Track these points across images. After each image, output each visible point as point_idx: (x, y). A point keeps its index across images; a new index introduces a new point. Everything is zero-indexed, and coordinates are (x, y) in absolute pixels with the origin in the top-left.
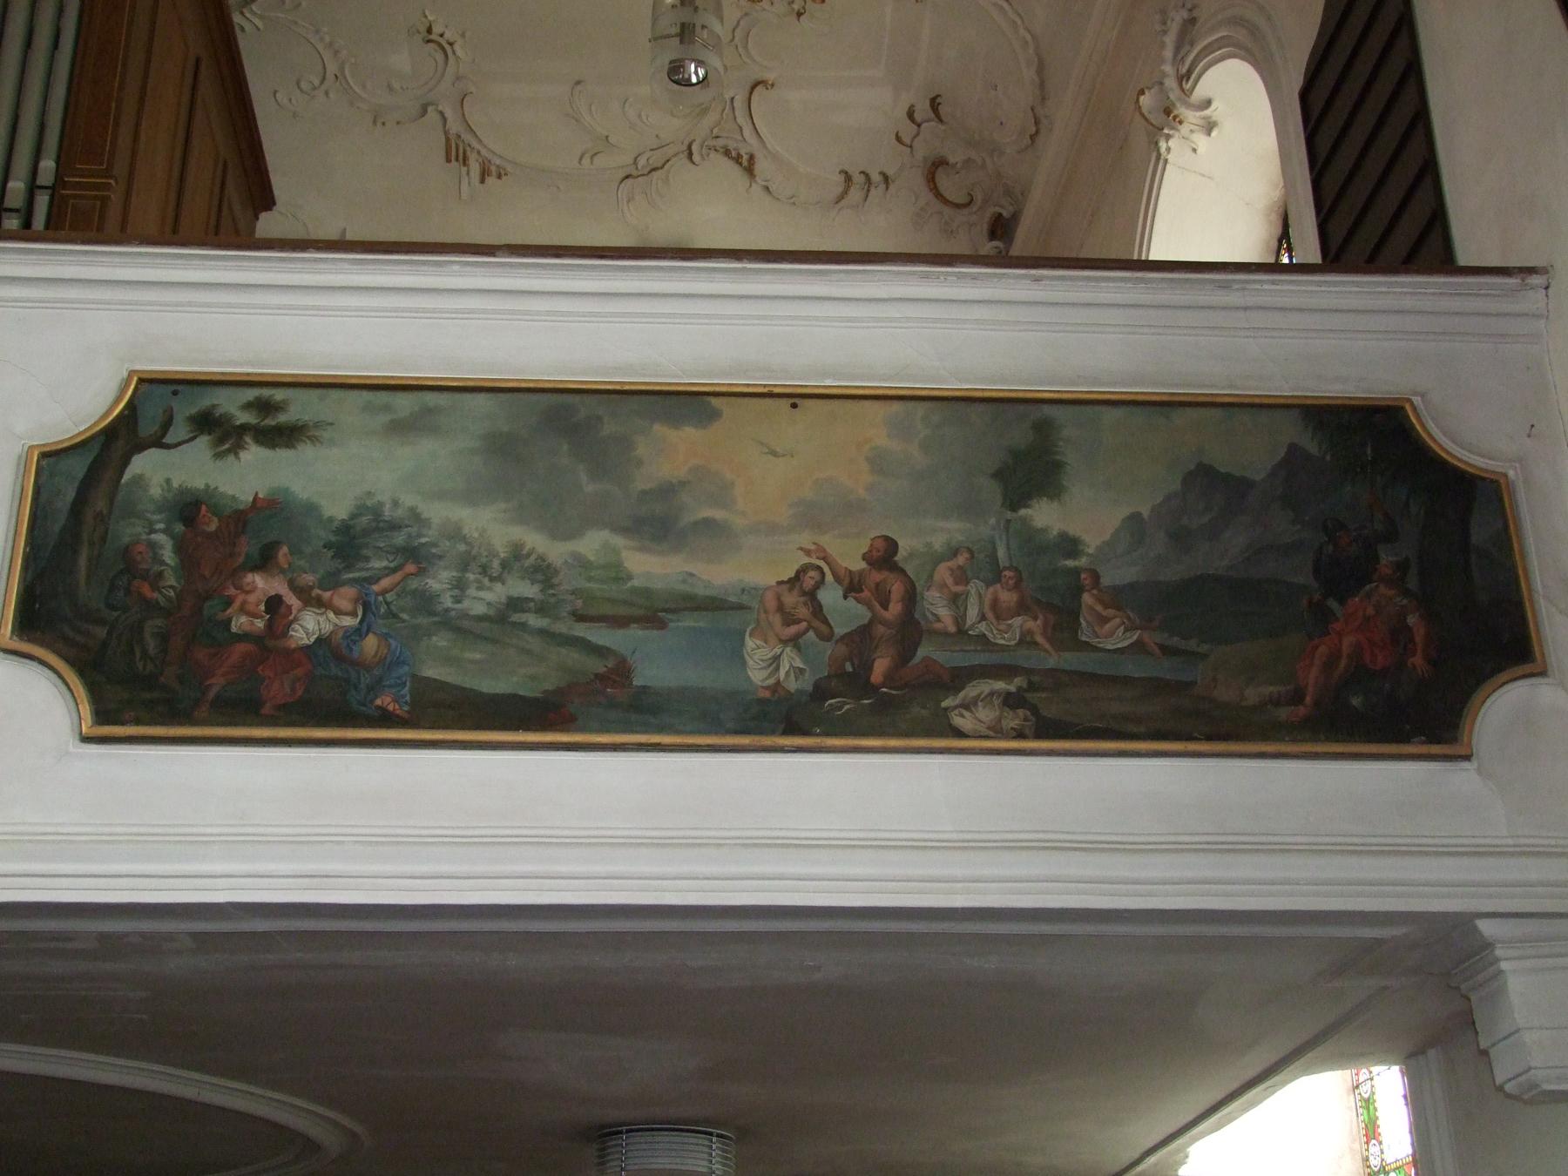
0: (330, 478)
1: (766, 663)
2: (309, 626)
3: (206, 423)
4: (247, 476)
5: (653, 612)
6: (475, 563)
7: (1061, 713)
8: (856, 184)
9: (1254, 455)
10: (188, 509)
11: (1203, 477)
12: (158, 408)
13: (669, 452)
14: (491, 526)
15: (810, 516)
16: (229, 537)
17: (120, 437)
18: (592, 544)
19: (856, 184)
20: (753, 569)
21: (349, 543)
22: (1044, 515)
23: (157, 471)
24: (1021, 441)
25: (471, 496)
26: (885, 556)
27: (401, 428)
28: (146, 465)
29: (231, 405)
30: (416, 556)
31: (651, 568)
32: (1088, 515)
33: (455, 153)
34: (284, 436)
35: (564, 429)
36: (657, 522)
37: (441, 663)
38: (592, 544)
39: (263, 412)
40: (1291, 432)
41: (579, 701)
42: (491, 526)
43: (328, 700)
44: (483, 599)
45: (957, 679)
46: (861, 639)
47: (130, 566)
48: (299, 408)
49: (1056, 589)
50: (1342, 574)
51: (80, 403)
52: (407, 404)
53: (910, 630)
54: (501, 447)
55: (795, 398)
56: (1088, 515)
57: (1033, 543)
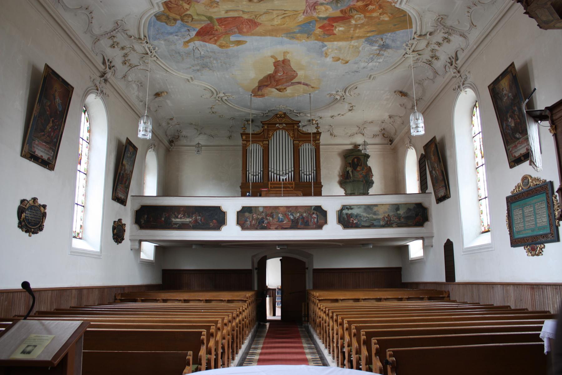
0: (355, 212)
1: (382, 223)
2: (355, 222)
3: (347, 208)
4: (350, 212)
5: (375, 220)
6: (364, 217)
7: (399, 225)
8: (375, 136)
9: (412, 207)
10: (347, 214)
11: (409, 210)
12: (344, 207)
13: (375, 209)
14: (365, 215)
15: (384, 213)
16: (349, 216)
17: (342, 210)
18: (371, 215)
19: (375, 136)
20: (380, 217)
21: (356, 216)
22: (398, 212)
23: (345, 212)
24: (397, 207)
25: (364, 212)
26: (389, 215)
27: (359, 208)
28: (344, 211)
29: (348, 207)
30: (360, 217)
31: (375, 217)
32: (401, 212)
33: (331, 134)
34: (352, 209)
35: (369, 208)
36: (375, 214)
37: (363, 224)
38: (371, 215)
39: (350, 207)
40: (414, 205)
41: (371, 226)
42: (365, 215)
43: (356, 226)
44: (365, 219)
45: (393, 223)
46: (387, 221)
47: (344, 218)
48: (352, 207)
49: (399, 217)
50: (417, 215)
51: (339, 208)
52: (359, 206)
53: (390, 220)
54: (365, 209)
55: (383, 205)
56: (401, 212)
57: (398, 214)
